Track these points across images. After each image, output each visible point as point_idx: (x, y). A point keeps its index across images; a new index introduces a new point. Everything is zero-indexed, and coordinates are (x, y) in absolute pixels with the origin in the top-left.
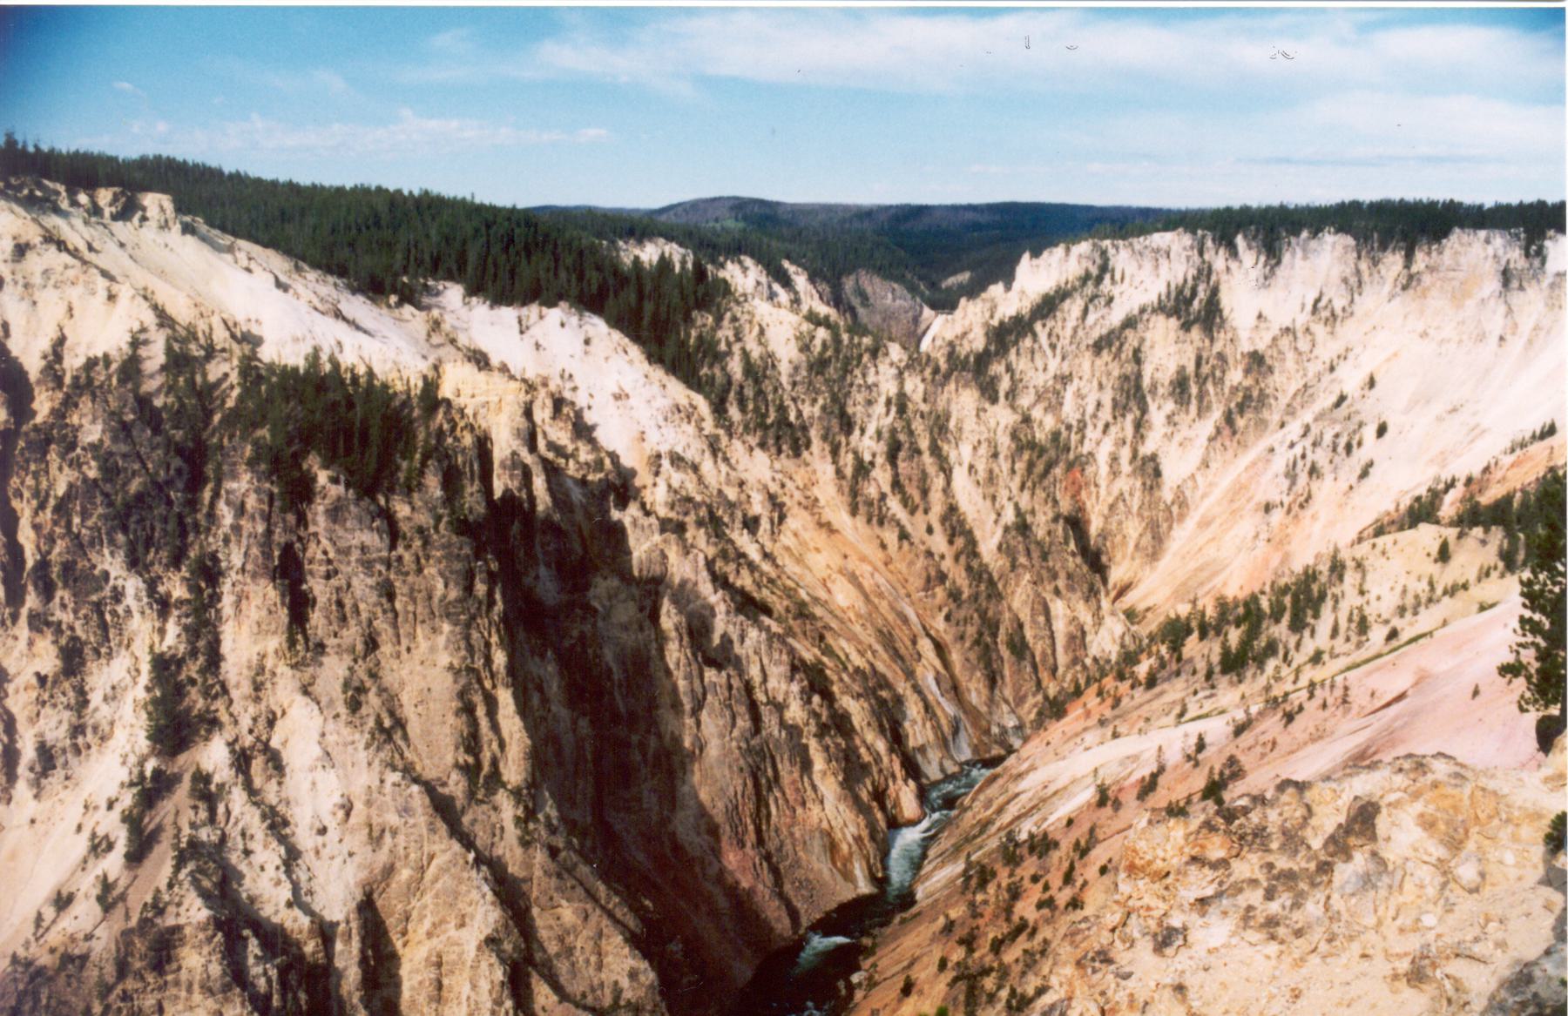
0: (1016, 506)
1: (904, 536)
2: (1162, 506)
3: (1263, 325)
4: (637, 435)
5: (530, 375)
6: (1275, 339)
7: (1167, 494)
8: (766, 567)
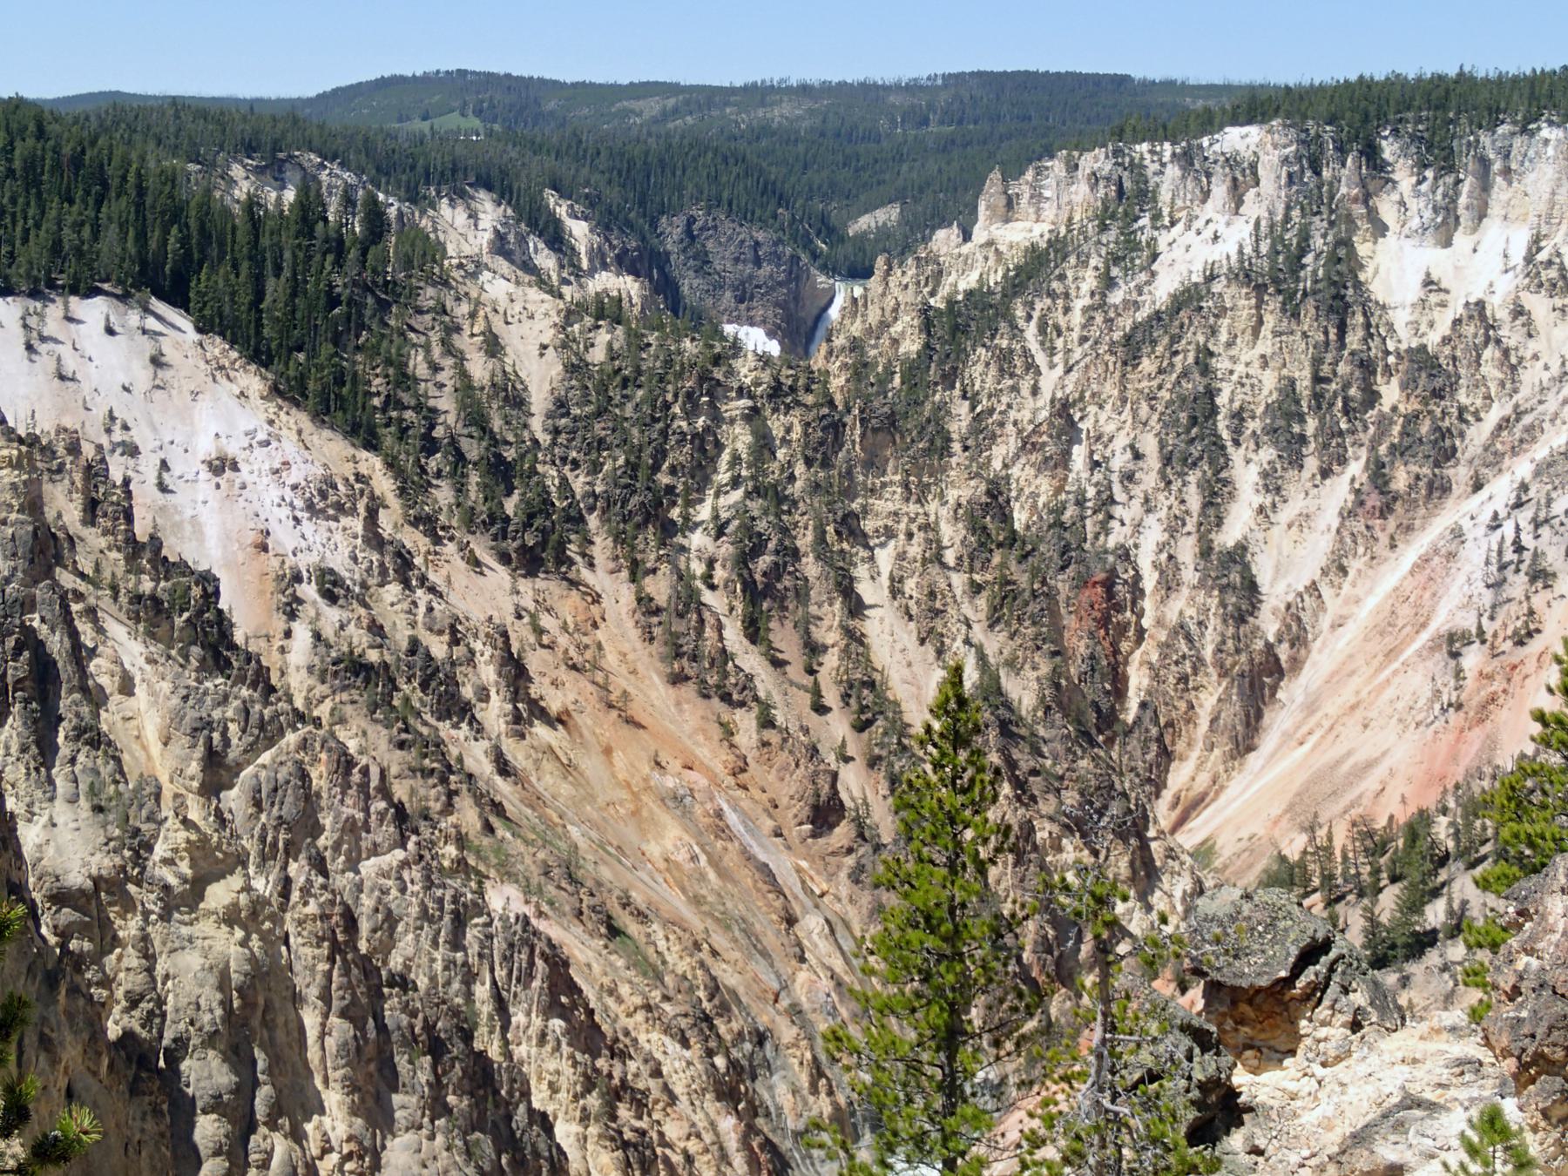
0: (982, 658)
1: (767, 722)
2: (1259, 645)
3: (1434, 298)
4: (252, 537)
5: (45, 426)
6: (1457, 322)
7: (1269, 624)
8: (504, 789)
